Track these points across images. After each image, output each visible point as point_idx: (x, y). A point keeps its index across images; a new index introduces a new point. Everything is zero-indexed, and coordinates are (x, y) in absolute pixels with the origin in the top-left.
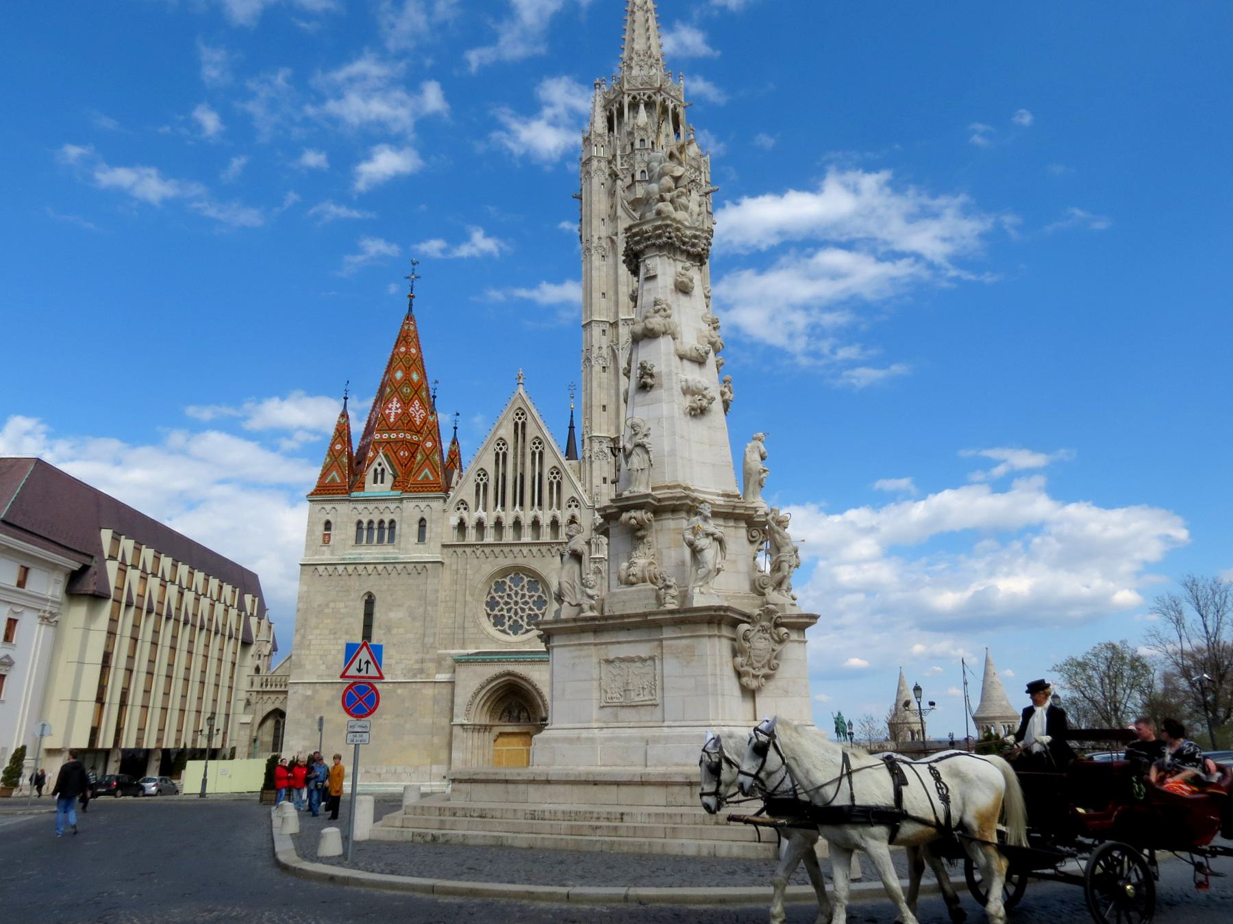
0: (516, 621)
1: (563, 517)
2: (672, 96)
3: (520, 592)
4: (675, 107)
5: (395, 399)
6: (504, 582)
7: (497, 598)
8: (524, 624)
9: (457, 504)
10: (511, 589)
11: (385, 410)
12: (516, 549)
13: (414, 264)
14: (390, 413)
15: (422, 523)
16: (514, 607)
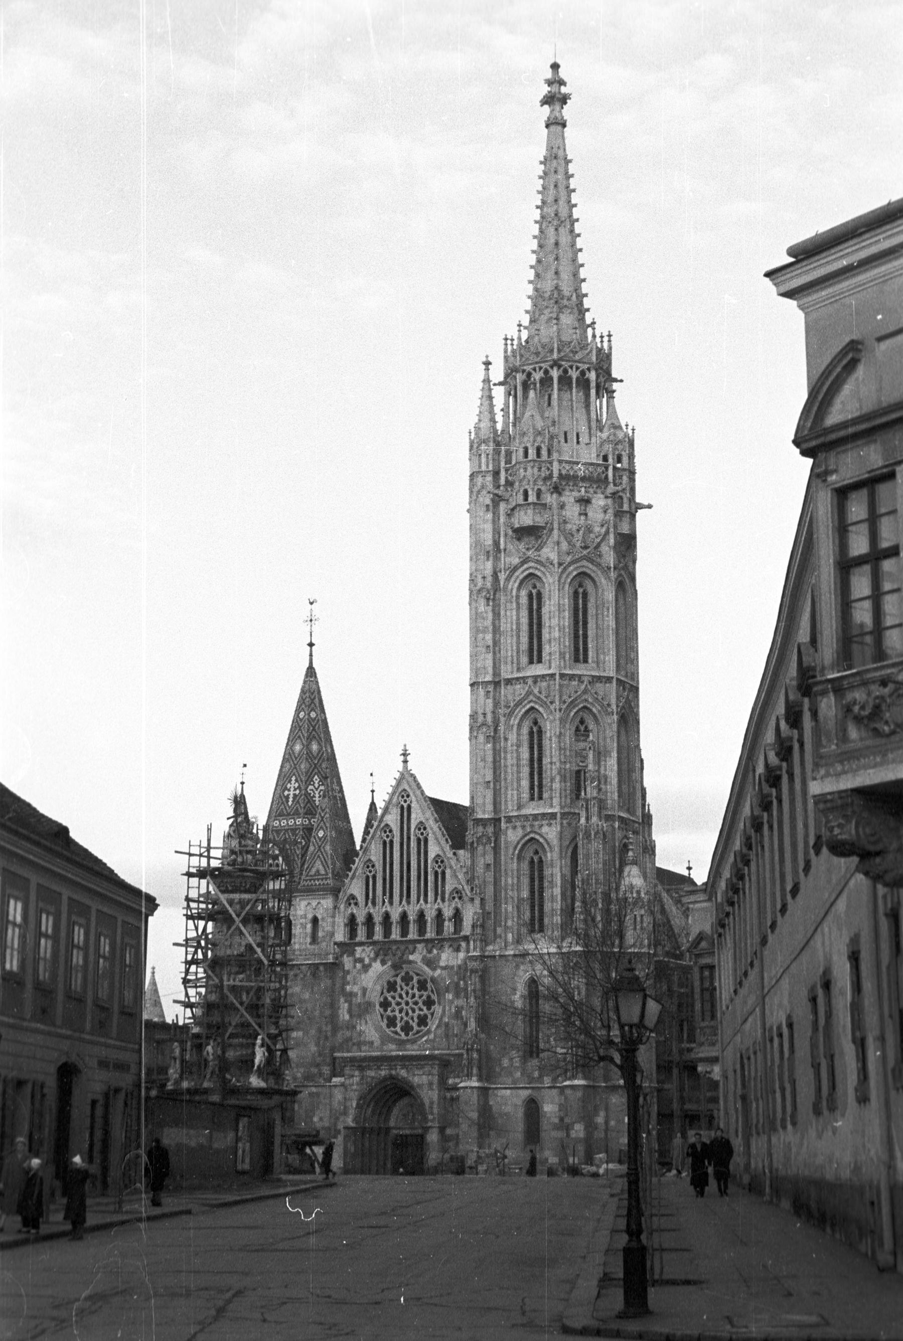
0: (407, 1023)
1: (448, 912)
2: (576, 361)
3: (410, 992)
4: (583, 373)
5: (293, 778)
6: (395, 982)
7: (390, 999)
8: (415, 1025)
9: (348, 899)
10: (402, 989)
11: (284, 791)
12: (403, 947)
13: (311, 603)
14: (288, 795)
15: (315, 921)
16: (405, 1007)
